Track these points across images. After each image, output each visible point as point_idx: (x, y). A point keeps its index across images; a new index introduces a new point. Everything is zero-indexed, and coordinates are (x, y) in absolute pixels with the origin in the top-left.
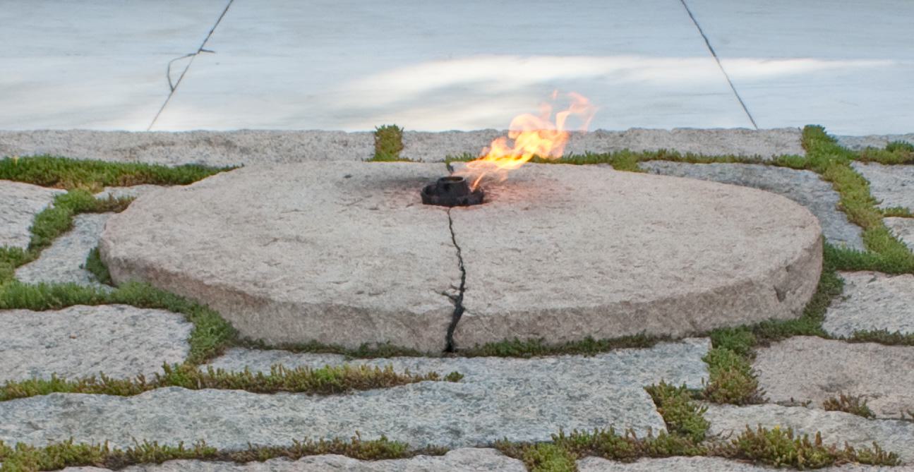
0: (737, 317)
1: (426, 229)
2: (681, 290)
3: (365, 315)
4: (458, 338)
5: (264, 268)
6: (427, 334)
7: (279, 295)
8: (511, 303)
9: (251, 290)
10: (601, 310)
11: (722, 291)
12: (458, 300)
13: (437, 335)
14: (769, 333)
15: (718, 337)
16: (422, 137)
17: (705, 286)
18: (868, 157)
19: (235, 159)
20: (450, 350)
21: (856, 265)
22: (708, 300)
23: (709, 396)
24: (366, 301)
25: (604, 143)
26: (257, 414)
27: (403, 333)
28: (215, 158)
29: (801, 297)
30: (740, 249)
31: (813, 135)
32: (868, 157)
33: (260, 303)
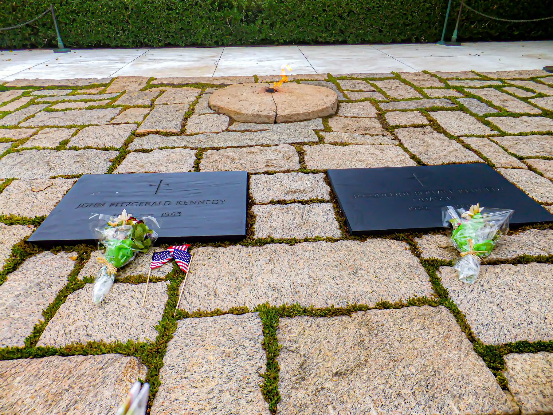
0: (326, 114)
1: (268, 98)
2: (316, 109)
3: (259, 116)
4: (277, 120)
5: (240, 107)
6: (271, 119)
7: (243, 112)
8: (286, 113)
9: (238, 111)
10: (302, 114)
11: (323, 109)
12: (276, 112)
13: (273, 119)
14: (331, 116)
15: (322, 118)
16: (262, 77)
17: (320, 108)
18: (339, 79)
19: (230, 82)
20: (275, 122)
21: (343, 101)
22: (322, 111)
23: (323, 131)
24: (260, 113)
25: (293, 77)
26: (243, 138)
27: (267, 119)
28: (226, 82)
29: (335, 109)
30: (325, 100)
31: (329, 75)
32: (339, 79)
33: (240, 114)
